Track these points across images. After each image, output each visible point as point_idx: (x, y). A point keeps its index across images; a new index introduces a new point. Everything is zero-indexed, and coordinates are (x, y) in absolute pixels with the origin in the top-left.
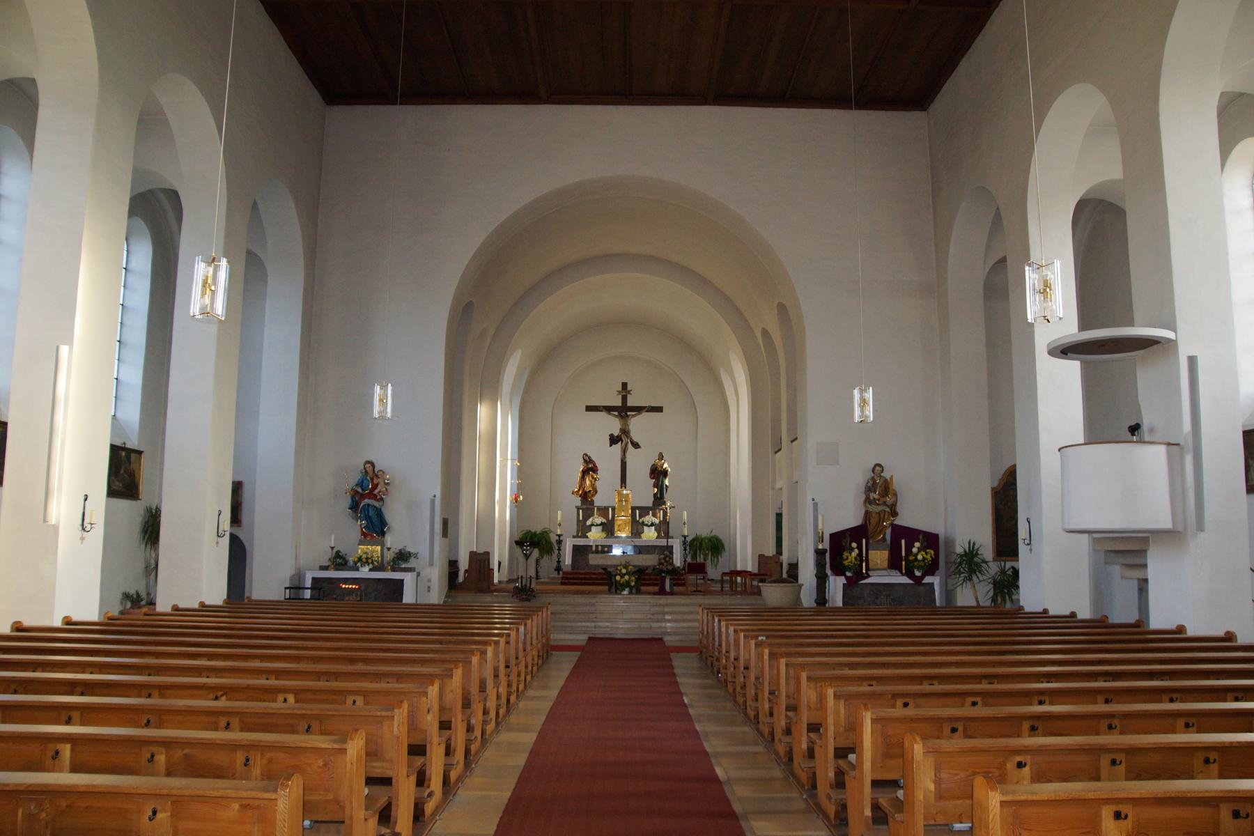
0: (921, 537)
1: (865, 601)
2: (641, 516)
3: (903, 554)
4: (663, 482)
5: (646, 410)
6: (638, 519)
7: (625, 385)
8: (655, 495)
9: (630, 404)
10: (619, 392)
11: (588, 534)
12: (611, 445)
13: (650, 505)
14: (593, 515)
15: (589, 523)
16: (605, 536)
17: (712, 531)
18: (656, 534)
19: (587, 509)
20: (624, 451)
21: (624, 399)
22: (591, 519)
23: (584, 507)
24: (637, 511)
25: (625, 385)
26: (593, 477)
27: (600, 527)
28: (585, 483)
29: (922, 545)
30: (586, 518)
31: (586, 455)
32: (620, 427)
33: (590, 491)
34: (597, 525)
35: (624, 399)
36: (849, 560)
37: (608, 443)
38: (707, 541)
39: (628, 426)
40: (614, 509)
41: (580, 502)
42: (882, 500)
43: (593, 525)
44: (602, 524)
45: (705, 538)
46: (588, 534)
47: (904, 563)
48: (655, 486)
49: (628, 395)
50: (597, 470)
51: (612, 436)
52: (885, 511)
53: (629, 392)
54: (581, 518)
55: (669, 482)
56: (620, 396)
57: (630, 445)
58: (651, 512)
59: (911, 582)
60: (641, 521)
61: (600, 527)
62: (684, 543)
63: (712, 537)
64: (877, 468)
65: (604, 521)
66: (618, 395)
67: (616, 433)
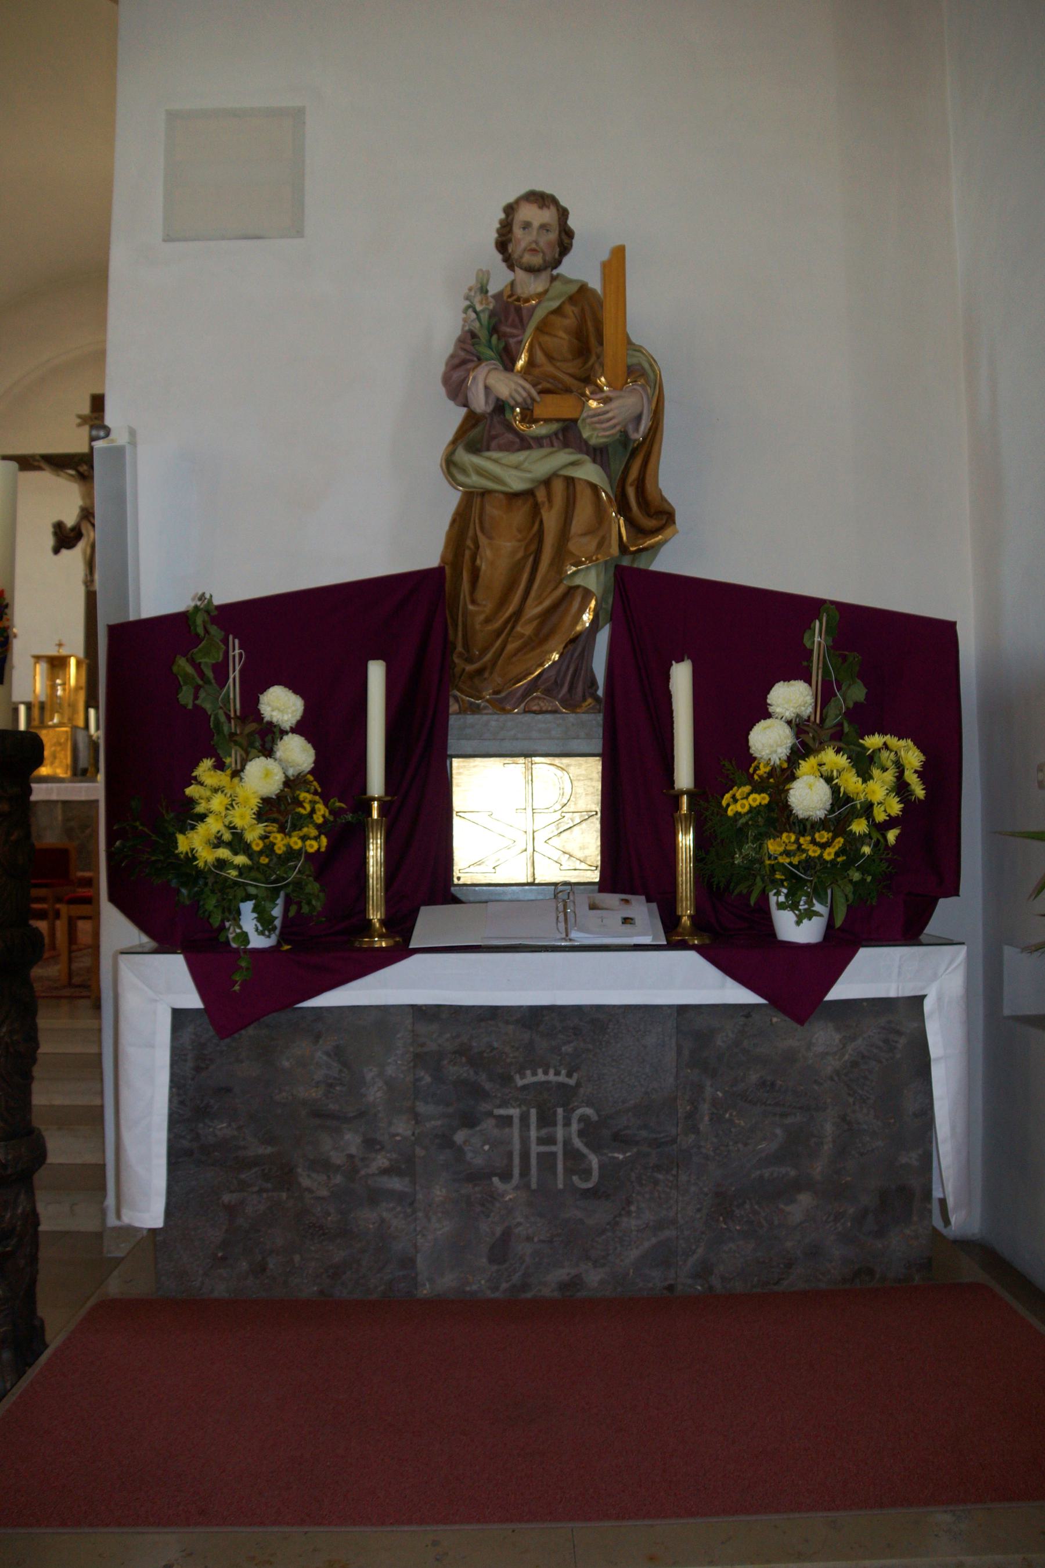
0: (817, 638)
1: (371, 1144)
3: (684, 776)
12: (56, 551)
29: (825, 696)
36: (213, 826)
42: (559, 407)
47: (686, 841)
51: (59, 528)
52: (570, 481)
59: (740, 995)
64: (529, 213)
66: (79, 425)
67: (70, 520)
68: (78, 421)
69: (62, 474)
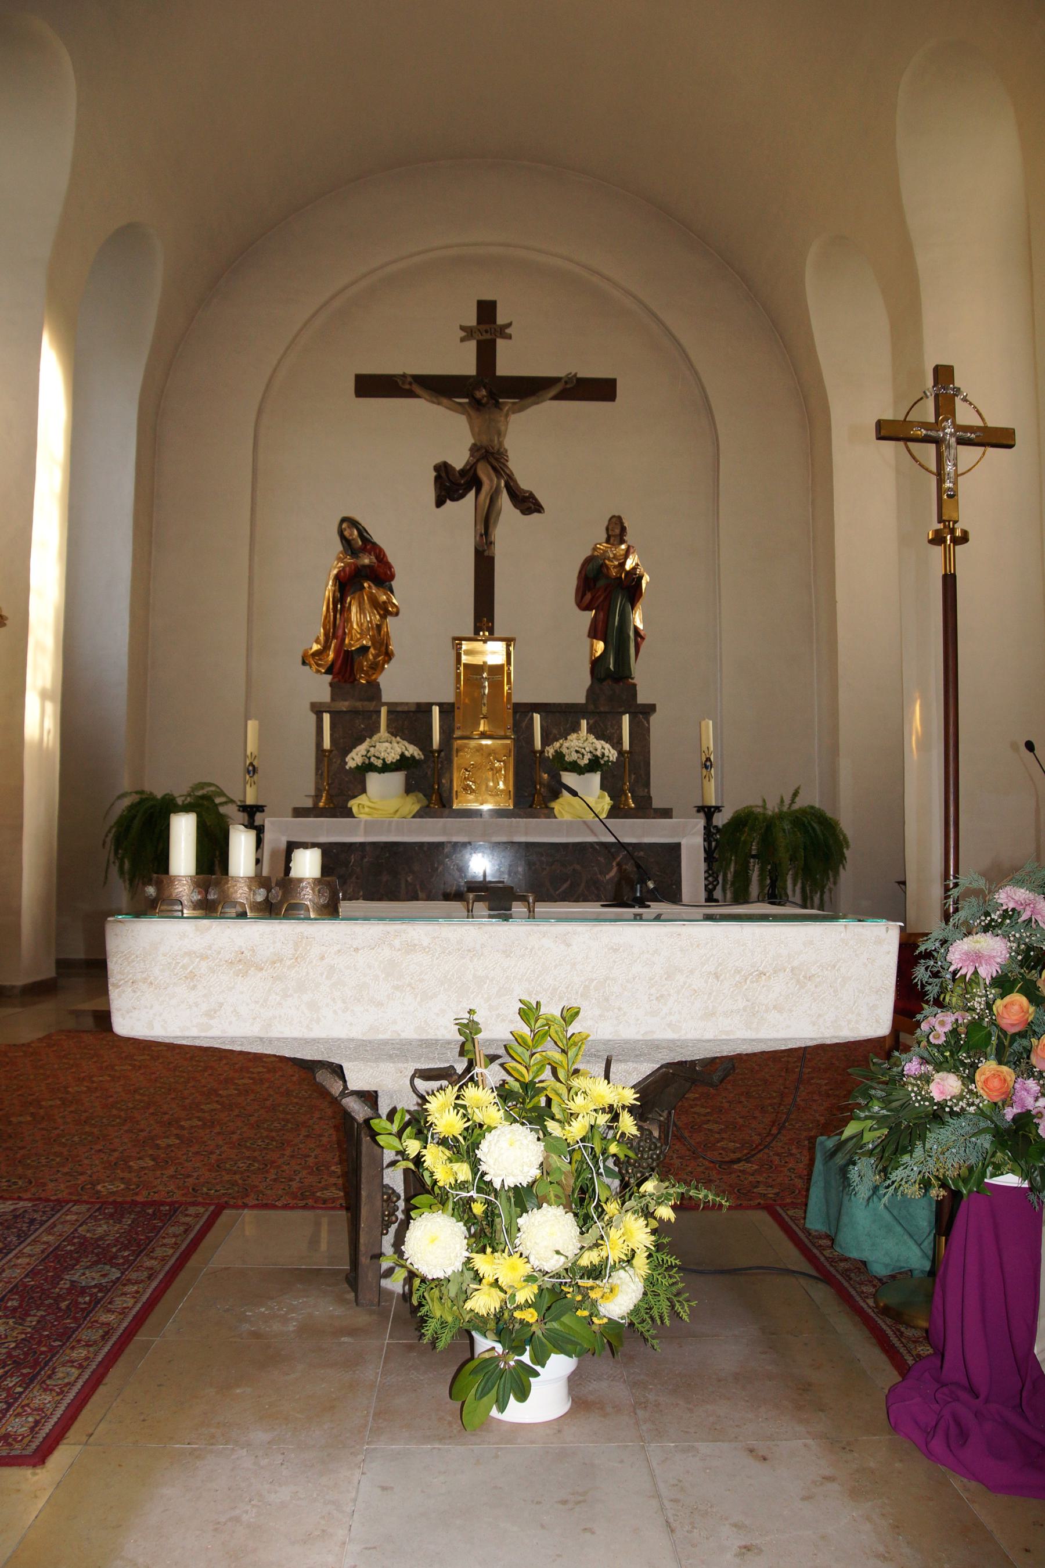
2: (546, 740)
4: (625, 620)
5: (553, 392)
6: (538, 744)
7: (487, 310)
8: (597, 664)
9: (503, 369)
10: (469, 333)
11: (353, 804)
12: (440, 503)
13: (579, 697)
14: (374, 729)
15: (355, 758)
16: (416, 808)
17: (796, 794)
18: (604, 803)
19: (354, 712)
20: (486, 522)
21: (486, 354)
22: (361, 749)
23: (344, 705)
24: (537, 717)
25: (487, 310)
26: (375, 604)
27: (397, 779)
28: (348, 620)
30: (345, 741)
31: (353, 523)
32: (470, 441)
33: (364, 649)
34: (386, 768)
35: (486, 354)
37: (430, 493)
38: (787, 826)
39: (499, 434)
40: (447, 710)
41: (328, 690)
43: (368, 767)
44: (403, 764)
45: (781, 816)
46: (353, 804)
48: (595, 633)
49: (500, 342)
50: (392, 577)
51: (443, 471)
53: (503, 332)
54: (327, 744)
55: (644, 621)
56: (472, 345)
57: (505, 499)
58: (584, 723)
60: (550, 751)
61: (397, 779)
62: (709, 832)
63: (803, 811)
65: (413, 751)
66: (462, 340)
67: (459, 460)
68: (463, 334)
69: (445, 401)
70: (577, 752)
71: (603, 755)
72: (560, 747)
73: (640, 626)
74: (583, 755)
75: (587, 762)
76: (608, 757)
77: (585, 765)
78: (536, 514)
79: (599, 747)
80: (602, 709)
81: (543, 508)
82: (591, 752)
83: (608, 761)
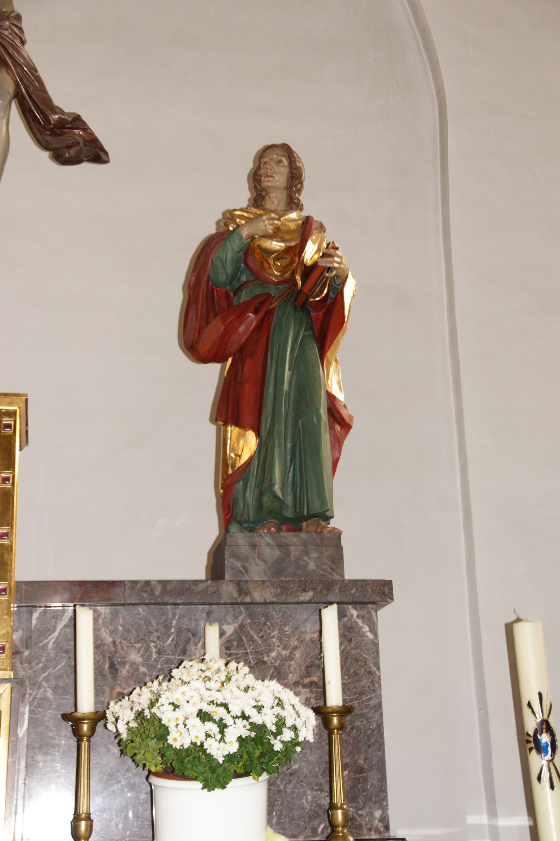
70: (204, 716)
71: (280, 723)
72: (152, 704)
73: (340, 396)
74: (222, 726)
75: (234, 748)
76: (294, 728)
77: (230, 758)
78: (86, 166)
79: (267, 700)
80: (257, 596)
81: (106, 153)
82: (244, 717)
83: (295, 743)
